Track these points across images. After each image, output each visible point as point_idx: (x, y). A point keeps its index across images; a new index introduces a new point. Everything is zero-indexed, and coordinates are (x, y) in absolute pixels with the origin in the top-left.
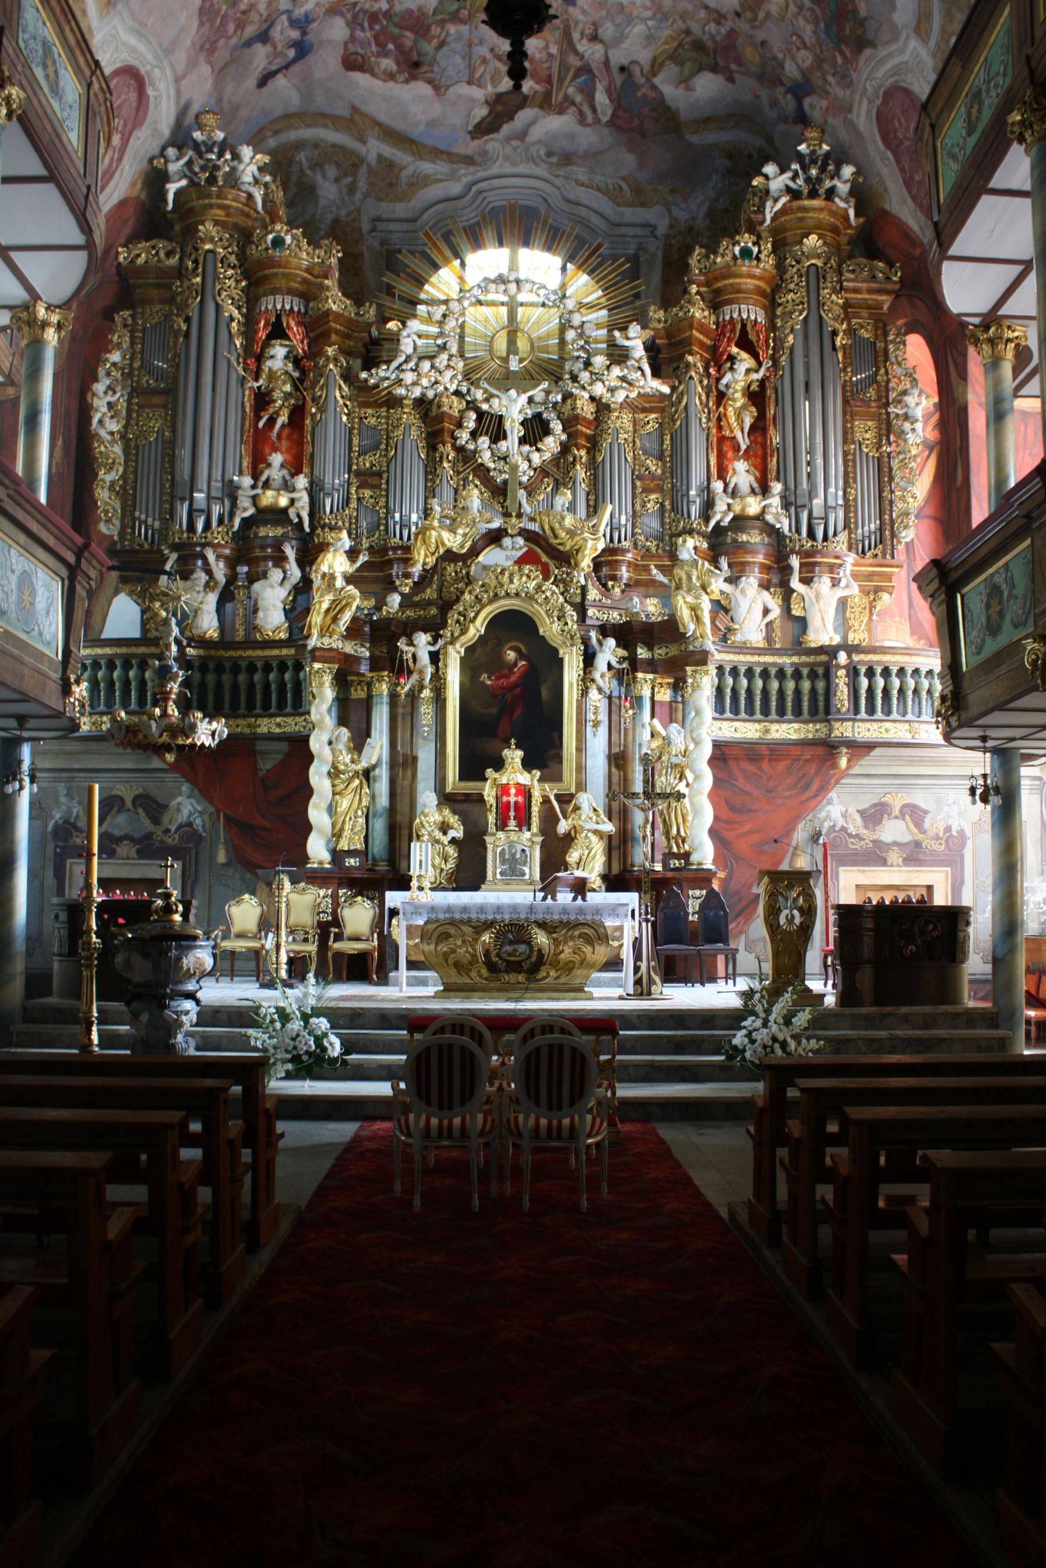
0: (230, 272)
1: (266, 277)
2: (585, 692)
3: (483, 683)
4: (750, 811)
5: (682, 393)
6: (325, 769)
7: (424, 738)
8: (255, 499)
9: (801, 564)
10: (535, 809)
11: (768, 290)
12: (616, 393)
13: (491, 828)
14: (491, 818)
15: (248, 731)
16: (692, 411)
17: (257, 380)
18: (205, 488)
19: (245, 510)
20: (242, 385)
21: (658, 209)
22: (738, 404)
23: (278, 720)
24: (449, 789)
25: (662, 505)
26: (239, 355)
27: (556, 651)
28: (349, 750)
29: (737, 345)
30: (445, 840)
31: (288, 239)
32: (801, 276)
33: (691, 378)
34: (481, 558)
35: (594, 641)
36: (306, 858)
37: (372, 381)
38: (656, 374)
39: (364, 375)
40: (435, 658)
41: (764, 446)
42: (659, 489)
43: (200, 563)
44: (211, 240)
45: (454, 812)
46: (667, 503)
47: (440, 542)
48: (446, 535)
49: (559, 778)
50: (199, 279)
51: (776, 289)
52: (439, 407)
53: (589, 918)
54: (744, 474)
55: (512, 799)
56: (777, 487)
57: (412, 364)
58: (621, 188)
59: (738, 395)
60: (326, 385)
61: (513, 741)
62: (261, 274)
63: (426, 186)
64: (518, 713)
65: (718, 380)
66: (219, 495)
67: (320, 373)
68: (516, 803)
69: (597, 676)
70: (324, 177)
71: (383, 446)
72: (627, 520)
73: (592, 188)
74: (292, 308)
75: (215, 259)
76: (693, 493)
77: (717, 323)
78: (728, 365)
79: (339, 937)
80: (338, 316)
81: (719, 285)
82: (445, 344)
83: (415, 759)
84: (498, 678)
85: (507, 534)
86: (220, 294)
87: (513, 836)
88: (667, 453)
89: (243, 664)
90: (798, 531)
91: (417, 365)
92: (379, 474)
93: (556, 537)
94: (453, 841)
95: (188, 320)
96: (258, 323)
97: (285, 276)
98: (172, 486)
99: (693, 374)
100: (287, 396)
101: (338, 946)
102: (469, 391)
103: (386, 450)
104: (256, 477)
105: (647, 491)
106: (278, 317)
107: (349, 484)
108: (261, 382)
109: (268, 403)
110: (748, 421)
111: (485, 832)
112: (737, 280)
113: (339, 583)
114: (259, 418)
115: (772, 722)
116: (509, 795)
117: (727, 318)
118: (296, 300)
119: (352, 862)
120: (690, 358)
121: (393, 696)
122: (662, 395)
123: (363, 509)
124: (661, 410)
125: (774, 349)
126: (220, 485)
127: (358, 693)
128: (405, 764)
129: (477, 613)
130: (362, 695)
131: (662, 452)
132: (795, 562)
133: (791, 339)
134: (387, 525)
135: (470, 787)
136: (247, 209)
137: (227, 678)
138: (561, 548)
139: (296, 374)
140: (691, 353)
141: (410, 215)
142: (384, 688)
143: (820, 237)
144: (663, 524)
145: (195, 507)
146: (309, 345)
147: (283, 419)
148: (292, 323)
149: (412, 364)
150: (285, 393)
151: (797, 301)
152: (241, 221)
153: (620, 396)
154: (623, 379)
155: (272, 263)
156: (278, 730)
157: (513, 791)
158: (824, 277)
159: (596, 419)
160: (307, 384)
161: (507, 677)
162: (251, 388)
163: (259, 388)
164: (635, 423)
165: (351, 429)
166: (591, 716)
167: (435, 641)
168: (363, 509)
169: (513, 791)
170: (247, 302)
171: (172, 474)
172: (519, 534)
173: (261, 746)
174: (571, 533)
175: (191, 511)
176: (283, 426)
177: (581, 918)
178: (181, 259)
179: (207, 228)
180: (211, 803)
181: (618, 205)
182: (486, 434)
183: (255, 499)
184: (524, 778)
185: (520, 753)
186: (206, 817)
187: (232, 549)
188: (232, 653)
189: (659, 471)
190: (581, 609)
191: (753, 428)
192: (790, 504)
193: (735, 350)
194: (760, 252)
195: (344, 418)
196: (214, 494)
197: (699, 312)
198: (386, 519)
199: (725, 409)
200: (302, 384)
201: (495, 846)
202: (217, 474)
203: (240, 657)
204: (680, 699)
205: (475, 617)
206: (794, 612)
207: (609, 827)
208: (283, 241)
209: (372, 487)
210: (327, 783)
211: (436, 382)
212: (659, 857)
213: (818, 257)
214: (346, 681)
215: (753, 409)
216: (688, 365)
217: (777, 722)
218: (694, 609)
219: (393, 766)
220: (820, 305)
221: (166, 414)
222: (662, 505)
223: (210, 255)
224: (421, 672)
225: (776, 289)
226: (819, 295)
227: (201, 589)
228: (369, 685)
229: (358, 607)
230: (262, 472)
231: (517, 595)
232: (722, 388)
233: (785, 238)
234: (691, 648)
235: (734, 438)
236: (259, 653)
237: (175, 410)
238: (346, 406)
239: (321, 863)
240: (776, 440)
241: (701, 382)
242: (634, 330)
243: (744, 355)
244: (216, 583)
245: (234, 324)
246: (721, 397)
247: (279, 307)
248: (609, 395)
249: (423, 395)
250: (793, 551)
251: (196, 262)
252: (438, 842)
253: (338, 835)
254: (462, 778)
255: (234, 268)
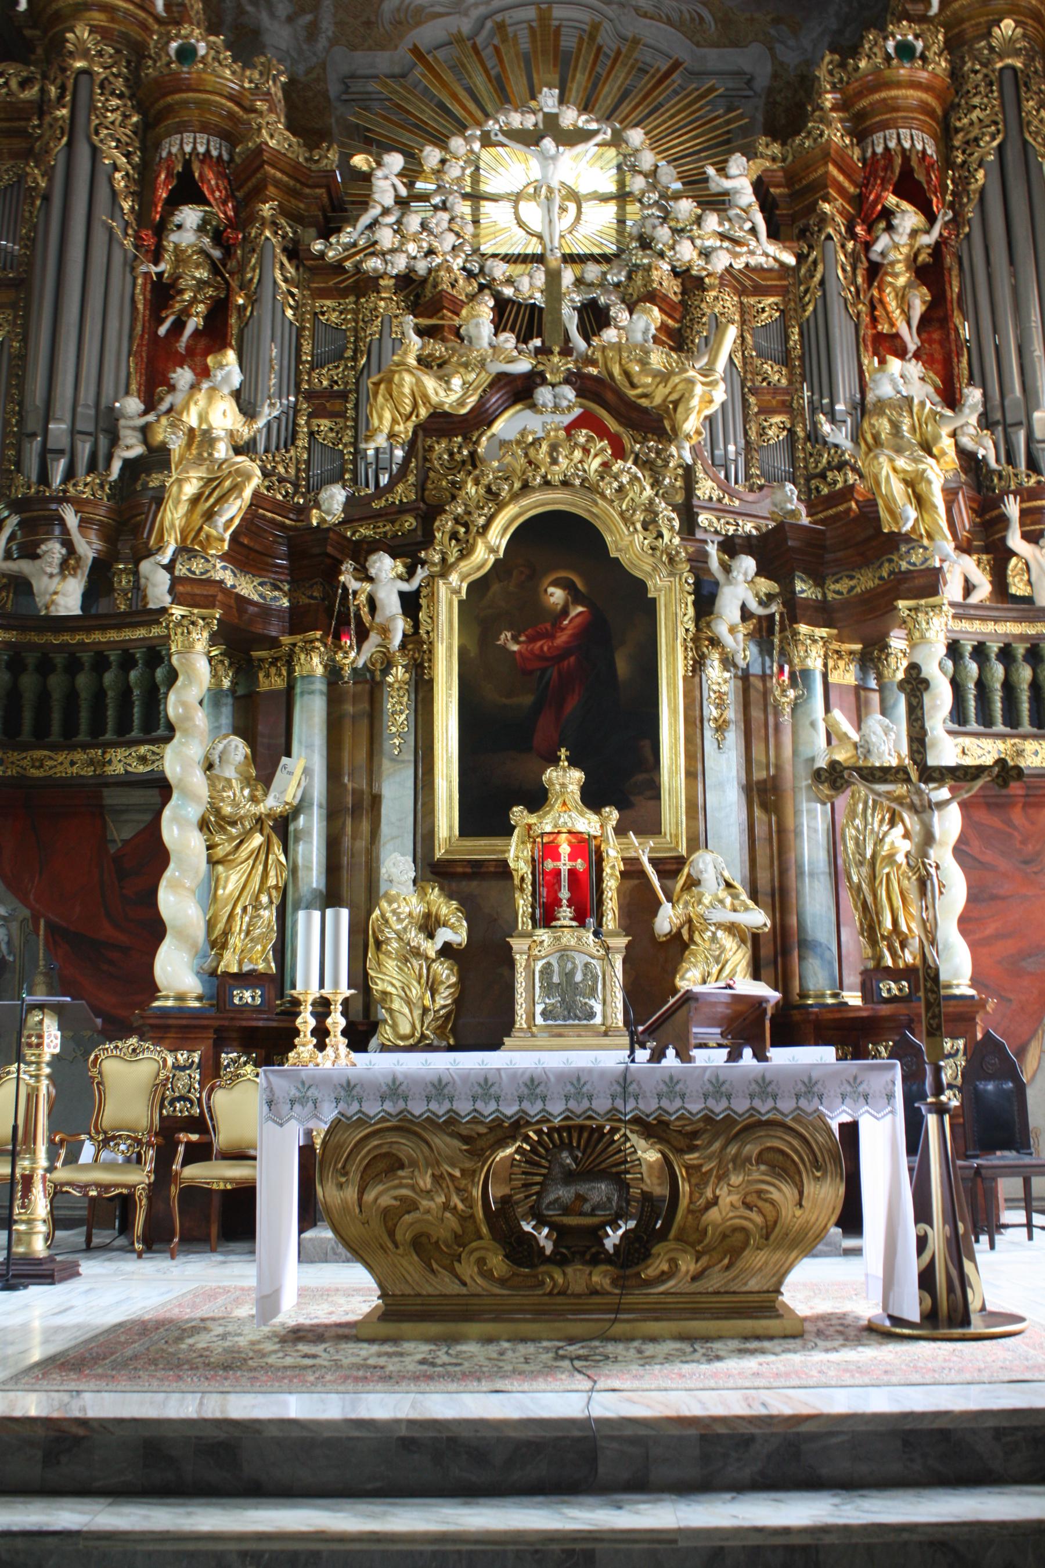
0: (115, 102)
1: (169, 109)
2: (698, 665)
3: (504, 648)
4: (994, 898)
5: (815, 263)
6: (194, 812)
7: (394, 760)
8: (145, 431)
9: (1023, 513)
10: (611, 884)
11: (939, 112)
12: (714, 258)
13: (524, 922)
14: (523, 904)
15: (89, 771)
16: (832, 287)
17: (156, 264)
18: (68, 416)
19: (128, 447)
20: (133, 269)
21: (756, 49)
22: (902, 281)
23: (143, 750)
24: (439, 854)
25: (791, 432)
26: (127, 224)
27: (641, 586)
28: (247, 781)
29: (895, 193)
30: (431, 948)
31: (202, 48)
32: (991, 84)
33: (829, 237)
34: (498, 426)
35: (714, 564)
36: (152, 989)
37: (331, 254)
38: (773, 234)
39: (318, 246)
40: (410, 603)
41: (945, 341)
42: (786, 408)
43: (57, 530)
44: (85, 54)
45: (450, 895)
46: (799, 430)
47: (419, 396)
48: (430, 383)
49: (651, 827)
50: (64, 112)
51: (951, 108)
52: (435, 285)
53: (786, 1105)
54: (918, 383)
55: (564, 865)
56: (974, 396)
57: (391, 219)
58: (702, 19)
59: (900, 267)
60: (260, 261)
61: (563, 753)
62: (162, 103)
63: (418, 24)
64: (572, 704)
65: (868, 246)
66: (91, 428)
67: (250, 245)
68: (572, 872)
69: (722, 629)
70: (272, 15)
71: (349, 353)
72: (737, 453)
73: (660, 20)
74: (208, 151)
75: (92, 81)
76: (840, 407)
77: (864, 160)
78: (882, 225)
79: (200, 1153)
80: (277, 159)
81: (864, 103)
82: (444, 202)
83: (376, 800)
84: (531, 640)
85: (544, 381)
86: (97, 134)
87: (568, 938)
88: (798, 352)
89: (86, 657)
90: (1011, 460)
91: (399, 222)
92: (344, 396)
93: (633, 386)
94: (447, 951)
95: (49, 173)
96: (159, 175)
97: (200, 104)
98: (20, 423)
99: (830, 231)
100: (201, 284)
101: (195, 1172)
102: (482, 269)
103: (354, 359)
104: (150, 405)
105: (766, 411)
106: (187, 164)
107: (296, 411)
108: (162, 267)
109: (173, 298)
110: (918, 309)
111: (511, 929)
112: (894, 93)
113: (222, 450)
114: (161, 321)
115: (1024, 737)
116: (557, 857)
117: (879, 150)
118: (215, 142)
119: (248, 996)
120: (826, 207)
121: (333, 672)
122: (782, 264)
123: (318, 449)
124: (783, 291)
125: (954, 193)
126: (92, 412)
127: (272, 682)
128: (356, 811)
129: (490, 519)
130: (278, 683)
131: (787, 352)
132: (1012, 508)
133: (980, 175)
134: (355, 472)
135: (481, 848)
136: (142, 14)
137: (56, 682)
138: (644, 402)
139: (217, 253)
140: (826, 199)
141: (397, 70)
142: (316, 665)
143: (1018, 23)
144: (793, 460)
145: (50, 445)
146: (234, 208)
147: (194, 323)
148: (210, 175)
149: (391, 219)
150: (200, 281)
151: (987, 122)
152: (135, 33)
153: (721, 261)
154: (723, 237)
155: (180, 85)
156: (142, 769)
157: (565, 849)
158: (1026, 85)
159: (682, 302)
160: (232, 264)
161: (552, 636)
162: (147, 274)
163: (160, 275)
164: (743, 309)
165: (300, 330)
166: (711, 711)
167: (411, 572)
168: (318, 449)
169: (565, 849)
170: (143, 149)
171: (21, 404)
172: (567, 381)
173: (112, 798)
174: (664, 377)
175: (45, 453)
176: (196, 333)
177: (764, 1107)
178: (43, 91)
179: (81, 33)
180: (24, 901)
181: (698, 44)
182: (512, 330)
183: (145, 431)
184: (587, 823)
185: (576, 777)
186: (15, 926)
187: (110, 510)
188: (66, 638)
189: (784, 381)
190: (688, 514)
191: (924, 319)
192: (997, 423)
193: (892, 200)
194: (926, 47)
195: (289, 313)
196: (80, 426)
197: (837, 136)
198: (354, 462)
199: (881, 290)
200: (224, 266)
201: (532, 959)
202: (87, 395)
203: (82, 644)
204: (873, 684)
205: (486, 527)
206: (1013, 590)
207: (757, 918)
208: (194, 50)
209: (331, 415)
210: (196, 841)
211: (431, 252)
212: (852, 978)
213: (1017, 53)
214: (250, 660)
215: (924, 290)
216: (823, 219)
217: (1035, 737)
218: (914, 484)
219: (333, 813)
220: (1022, 125)
221: (16, 317)
222: (791, 432)
223: (84, 78)
224: (385, 631)
225: (951, 108)
226: (1020, 109)
227: (56, 570)
228: (290, 662)
229: (256, 494)
230: (161, 399)
231: (566, 483)
232: (875, 257)
233: (961, 34)
234: (904, 566)
235: (897, 336)
236: (113, 636)
237: (27, 308)
238: (293, 295)
239: (180, 997)
240: (966, 332)
241: (843, 246)
242: (737, 163)
243: (905, 205)
244: (79, 559)
245: (118, 175)
246: (875, 271)
247: (188, 149)
248: (702, 263)
249: (411, 270)
250: (1007, 493)
251: (63, 88)
252: (417, 953)
253: (218, 944)
254: (465, 829)
255: (120, 97)
